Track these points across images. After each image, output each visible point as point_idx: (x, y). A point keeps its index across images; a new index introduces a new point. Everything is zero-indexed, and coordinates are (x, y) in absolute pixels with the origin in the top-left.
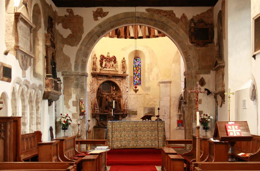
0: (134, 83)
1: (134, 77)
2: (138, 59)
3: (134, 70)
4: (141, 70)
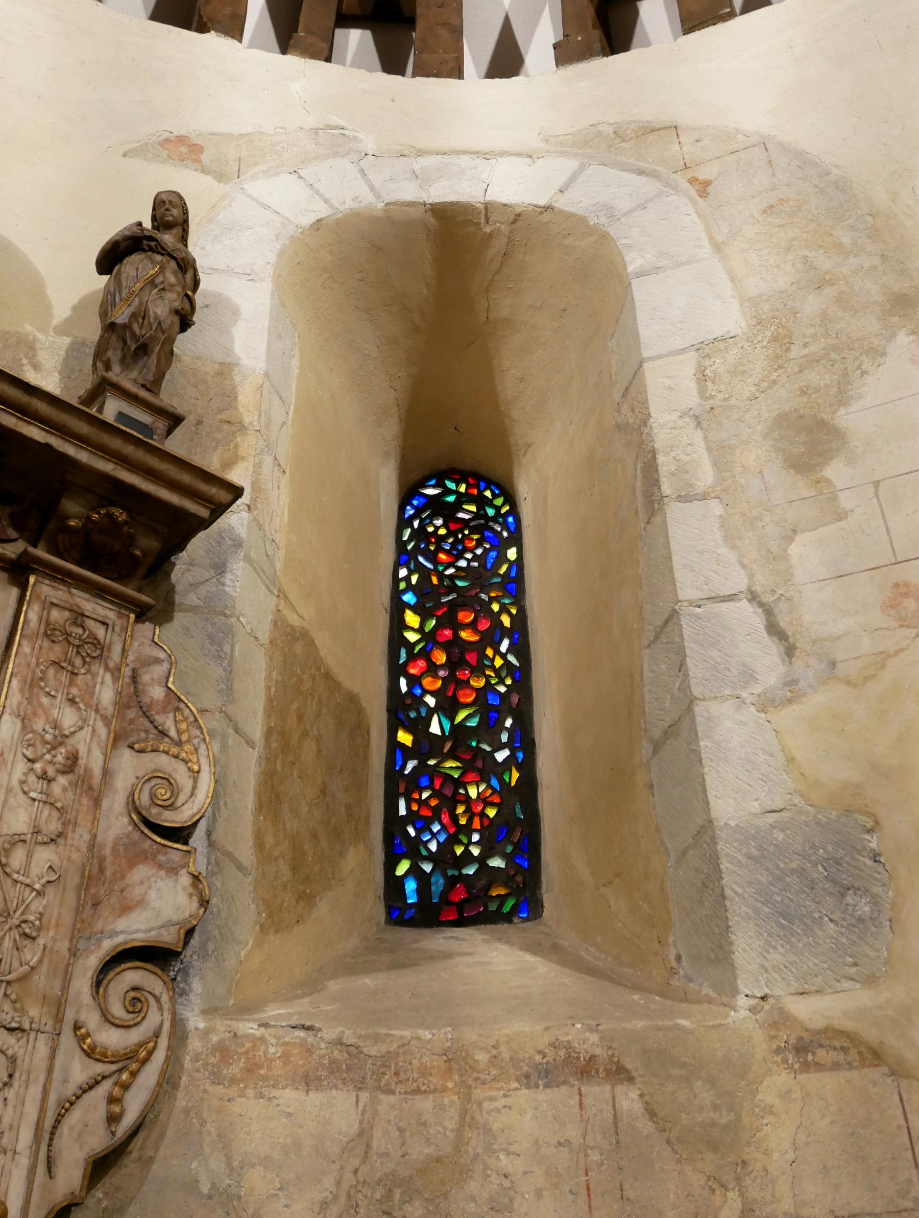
0: (394, 886)
1: (393, 775)
2: (482, 502)
3: (396, 639)
4: (521, 647)
